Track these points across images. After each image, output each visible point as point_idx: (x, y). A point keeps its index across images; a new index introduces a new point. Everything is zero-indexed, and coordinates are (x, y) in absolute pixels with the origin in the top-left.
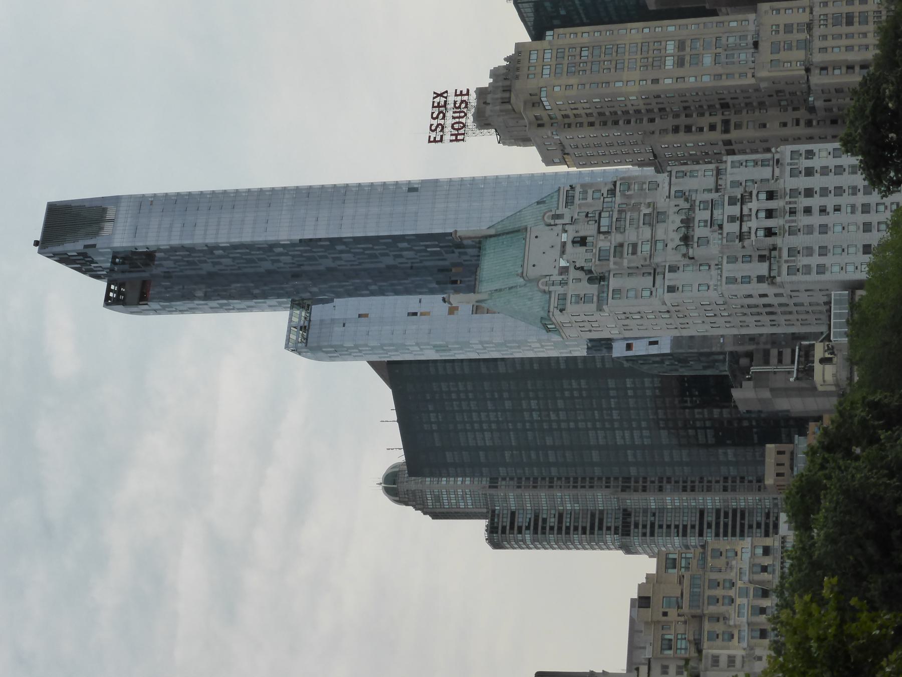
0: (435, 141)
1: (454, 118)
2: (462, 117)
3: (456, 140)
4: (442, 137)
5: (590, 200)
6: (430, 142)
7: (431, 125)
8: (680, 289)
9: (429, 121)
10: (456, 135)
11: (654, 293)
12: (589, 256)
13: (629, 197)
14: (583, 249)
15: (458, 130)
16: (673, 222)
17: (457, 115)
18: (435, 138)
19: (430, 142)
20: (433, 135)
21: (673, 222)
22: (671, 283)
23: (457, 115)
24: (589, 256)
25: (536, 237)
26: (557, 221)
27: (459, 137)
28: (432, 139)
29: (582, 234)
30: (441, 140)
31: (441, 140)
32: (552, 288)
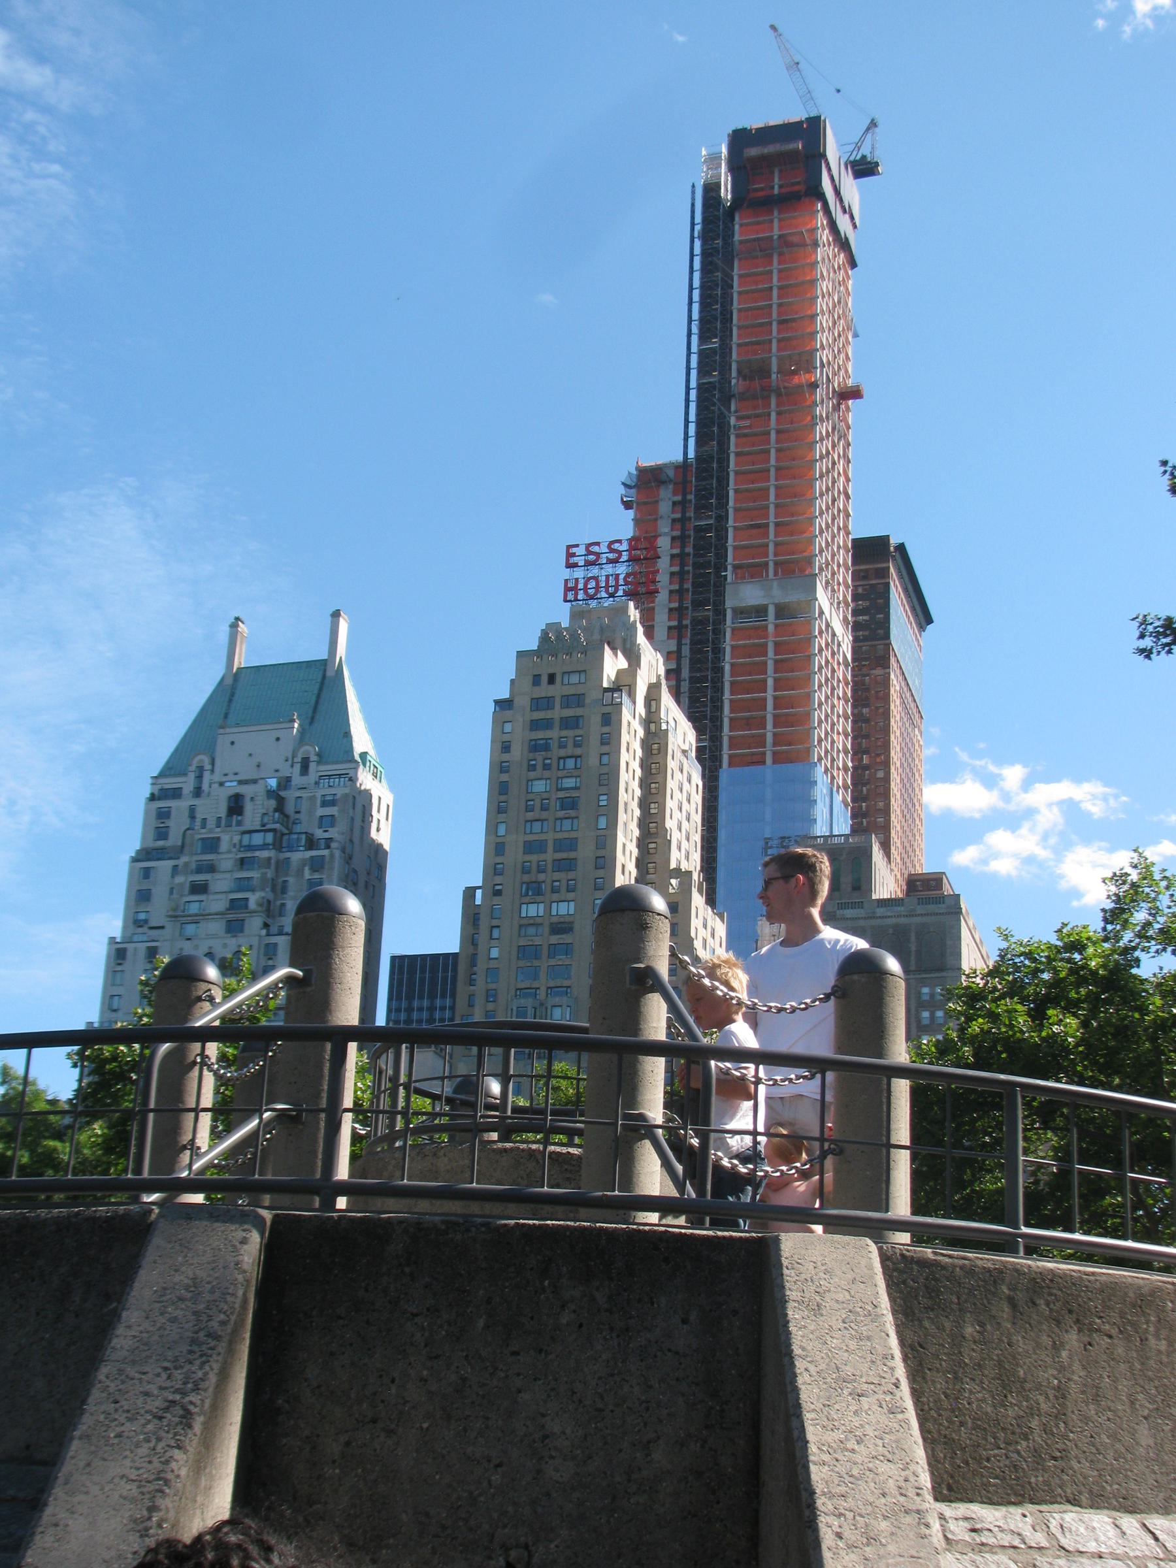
0: (570, 555)
1: (607, 577)
2: (607, 591)
3: (567, 589)
4: (575, 565)
5: (321, 811)
6: (569, 547)
7: (598, 544)
8: (119, 968)
9: (605, 537)
10: (575, 589)
11: (140, 930)
12: (211, 823)
13: (300, 872)
14: (222, 811)
15: (585, 589)
16: (225, 946)
17: (612, 582)
18: (574, 555)
19: (569, 547)
20: (581, 551)
21: (225, 946)
22: (129, 954)
23: (612, 582)
24: (211, 823)
25: (278, 739)
26: (298, 767)
27: (570, 596)
28: (574, 550)
29: (248, 807)
30: (570, 566)
31: (570, 566)
32: (192, 776)
